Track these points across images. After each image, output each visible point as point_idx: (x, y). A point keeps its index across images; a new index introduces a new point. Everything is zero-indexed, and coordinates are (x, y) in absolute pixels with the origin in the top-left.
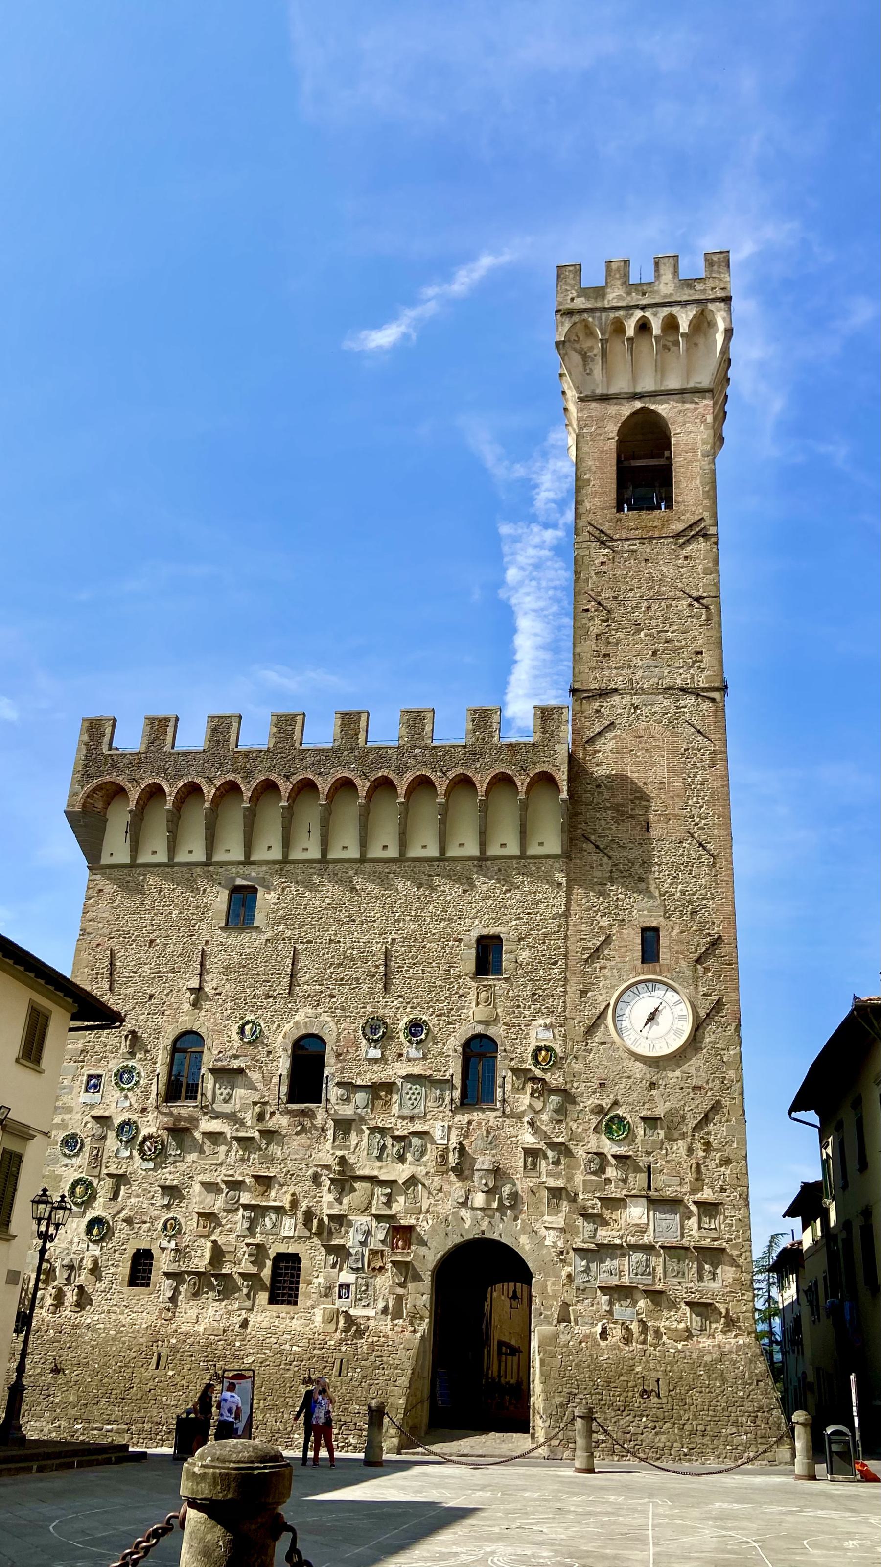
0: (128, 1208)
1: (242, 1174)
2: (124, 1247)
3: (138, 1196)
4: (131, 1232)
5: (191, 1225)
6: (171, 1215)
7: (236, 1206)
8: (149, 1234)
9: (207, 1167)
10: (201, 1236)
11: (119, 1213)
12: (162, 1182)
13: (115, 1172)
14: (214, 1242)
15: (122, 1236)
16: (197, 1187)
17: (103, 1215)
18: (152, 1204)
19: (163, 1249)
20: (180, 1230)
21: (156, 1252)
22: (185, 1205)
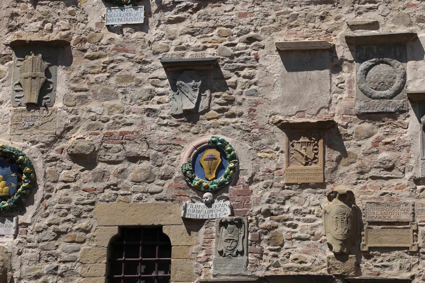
0: (84, 125)
1: (399, 20)
2: (83, 224)
3: (108, 95)
4: (100, 185)
5: (266, 160)
6: (208, 138)
7: (399, 101)
8: (153, 187)
9: (295, 10)
10: (304, 186)
11: (59, 138)
12: (173, 55)
13: (36, 37)
14: (347, 198)
15: (75, 197)
16: (274, 64)
17: (17, 145)
18: (151, 112)
19: (193, 225)
20: (236, 170)
21: (176, 234)
22: (244, 109)
